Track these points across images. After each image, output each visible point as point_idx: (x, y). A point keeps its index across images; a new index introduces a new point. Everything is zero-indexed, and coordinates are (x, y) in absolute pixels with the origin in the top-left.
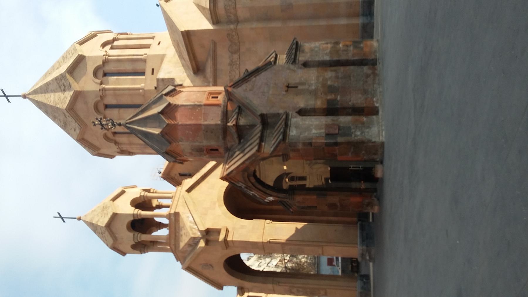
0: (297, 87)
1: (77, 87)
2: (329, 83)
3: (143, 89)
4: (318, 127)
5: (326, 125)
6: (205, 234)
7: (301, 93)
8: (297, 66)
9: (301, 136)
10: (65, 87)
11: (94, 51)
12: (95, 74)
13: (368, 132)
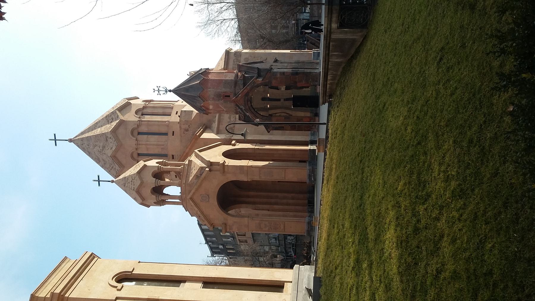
1: (121, 117)
3: (168, 121)
6: (210, 164)
10: (112, 119)
11: (138, 103)
12: (136, 112)
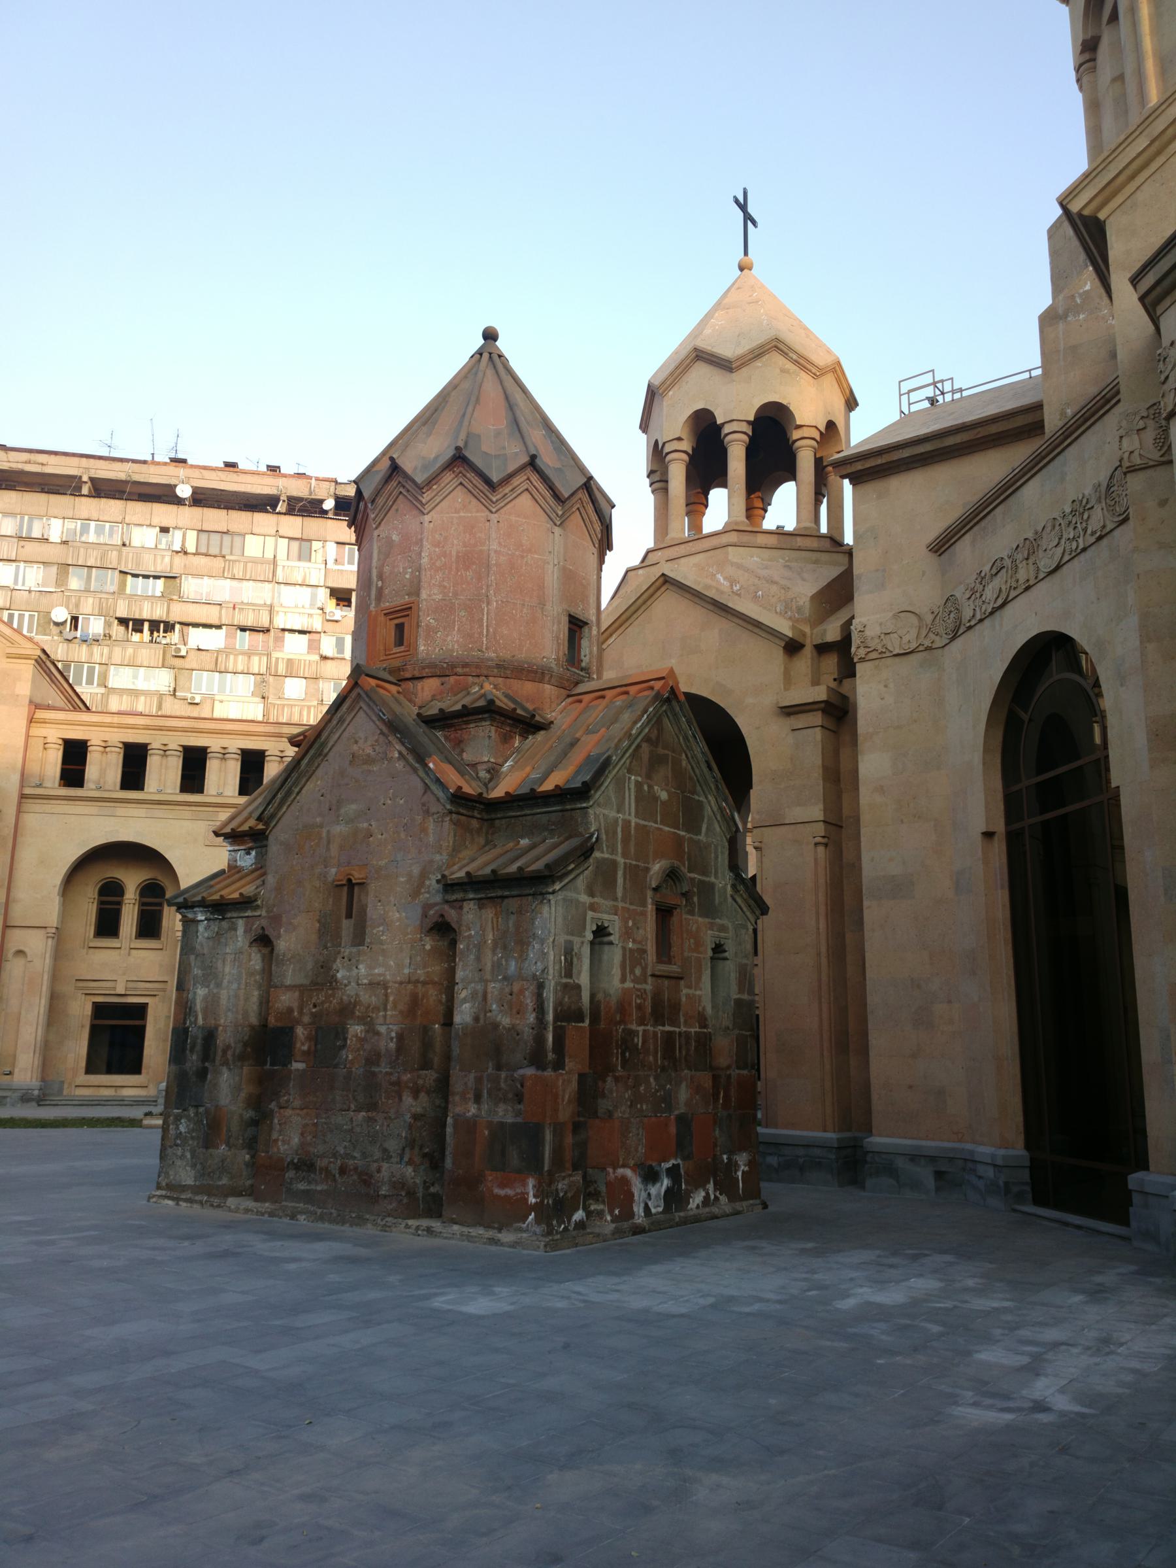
0: (349, 915)
2: (356, 1029)
4: (212, 1004)
5: (216, 1028)
7: (327, 933)
8: (438, 898)
9: (192, 957)
13: (182, 1157)
